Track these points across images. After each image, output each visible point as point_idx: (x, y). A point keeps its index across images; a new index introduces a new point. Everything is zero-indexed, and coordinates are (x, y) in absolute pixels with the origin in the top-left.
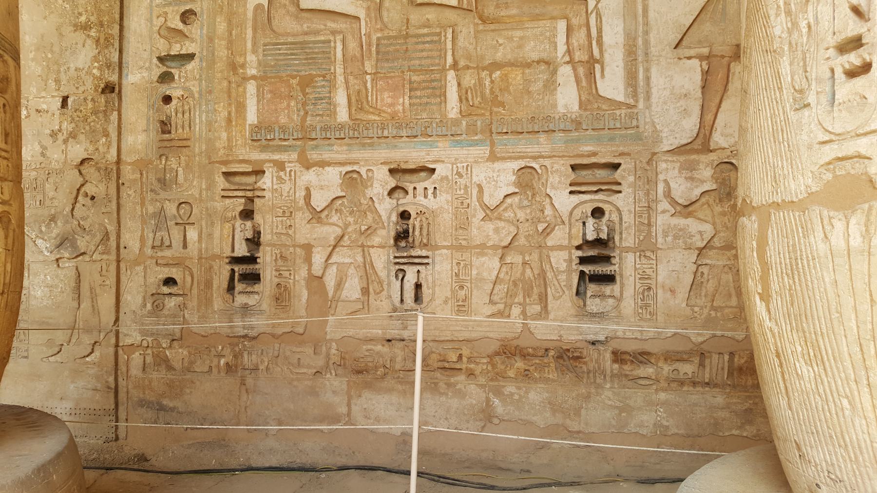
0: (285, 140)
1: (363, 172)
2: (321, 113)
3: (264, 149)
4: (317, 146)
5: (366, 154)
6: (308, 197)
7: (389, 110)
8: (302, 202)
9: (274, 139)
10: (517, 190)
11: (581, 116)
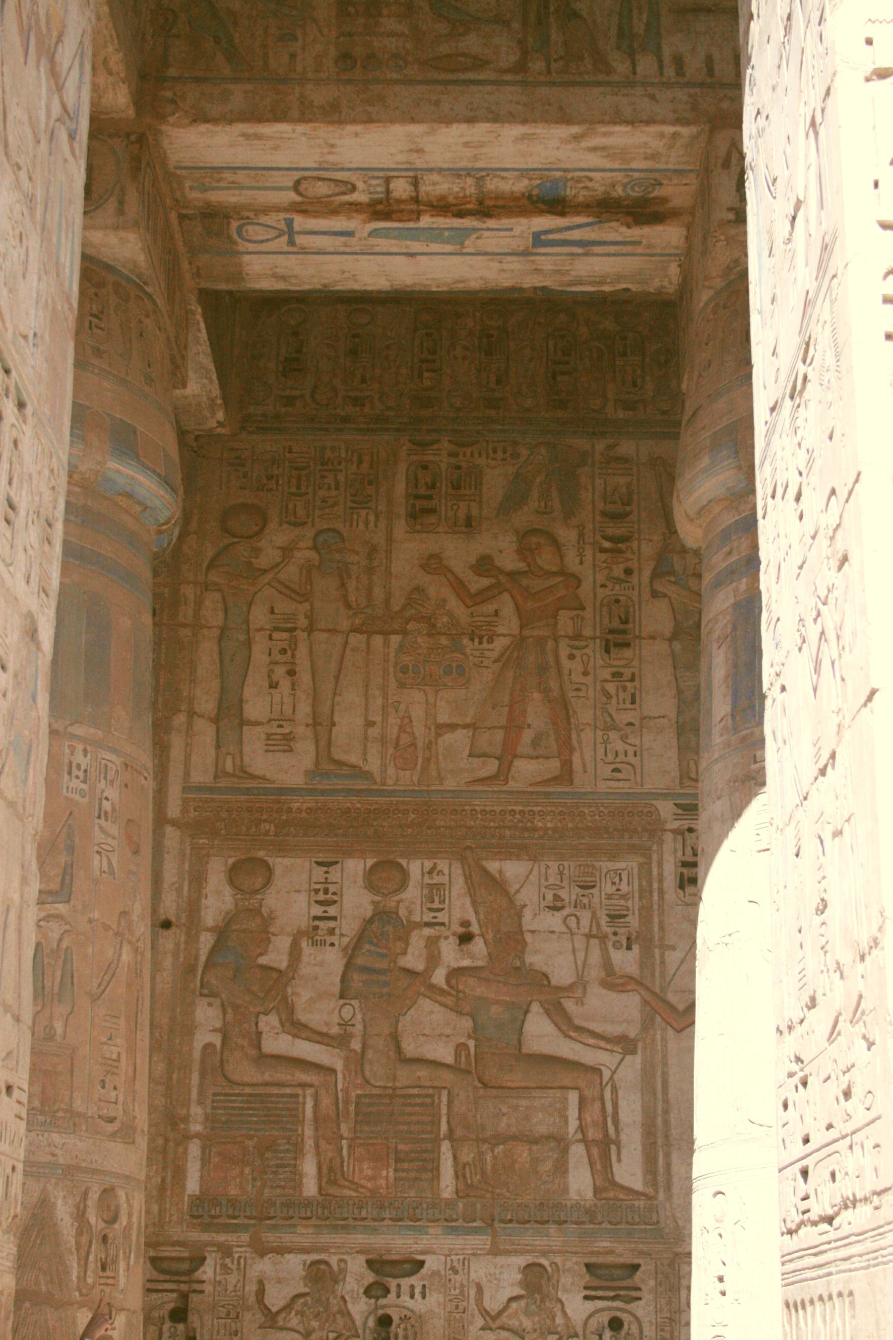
0: (234, 1218)
1: (334, 1260)
2: (283, 1184)
3: (207, 1227)
4: (275, 1227)
5: (339, 1238)
6: (261, 1292)
7: (369, 1185)
8: (252, 1299)
9: (220, 1216)
10: (523, 1292)
11: (595, 1205)
